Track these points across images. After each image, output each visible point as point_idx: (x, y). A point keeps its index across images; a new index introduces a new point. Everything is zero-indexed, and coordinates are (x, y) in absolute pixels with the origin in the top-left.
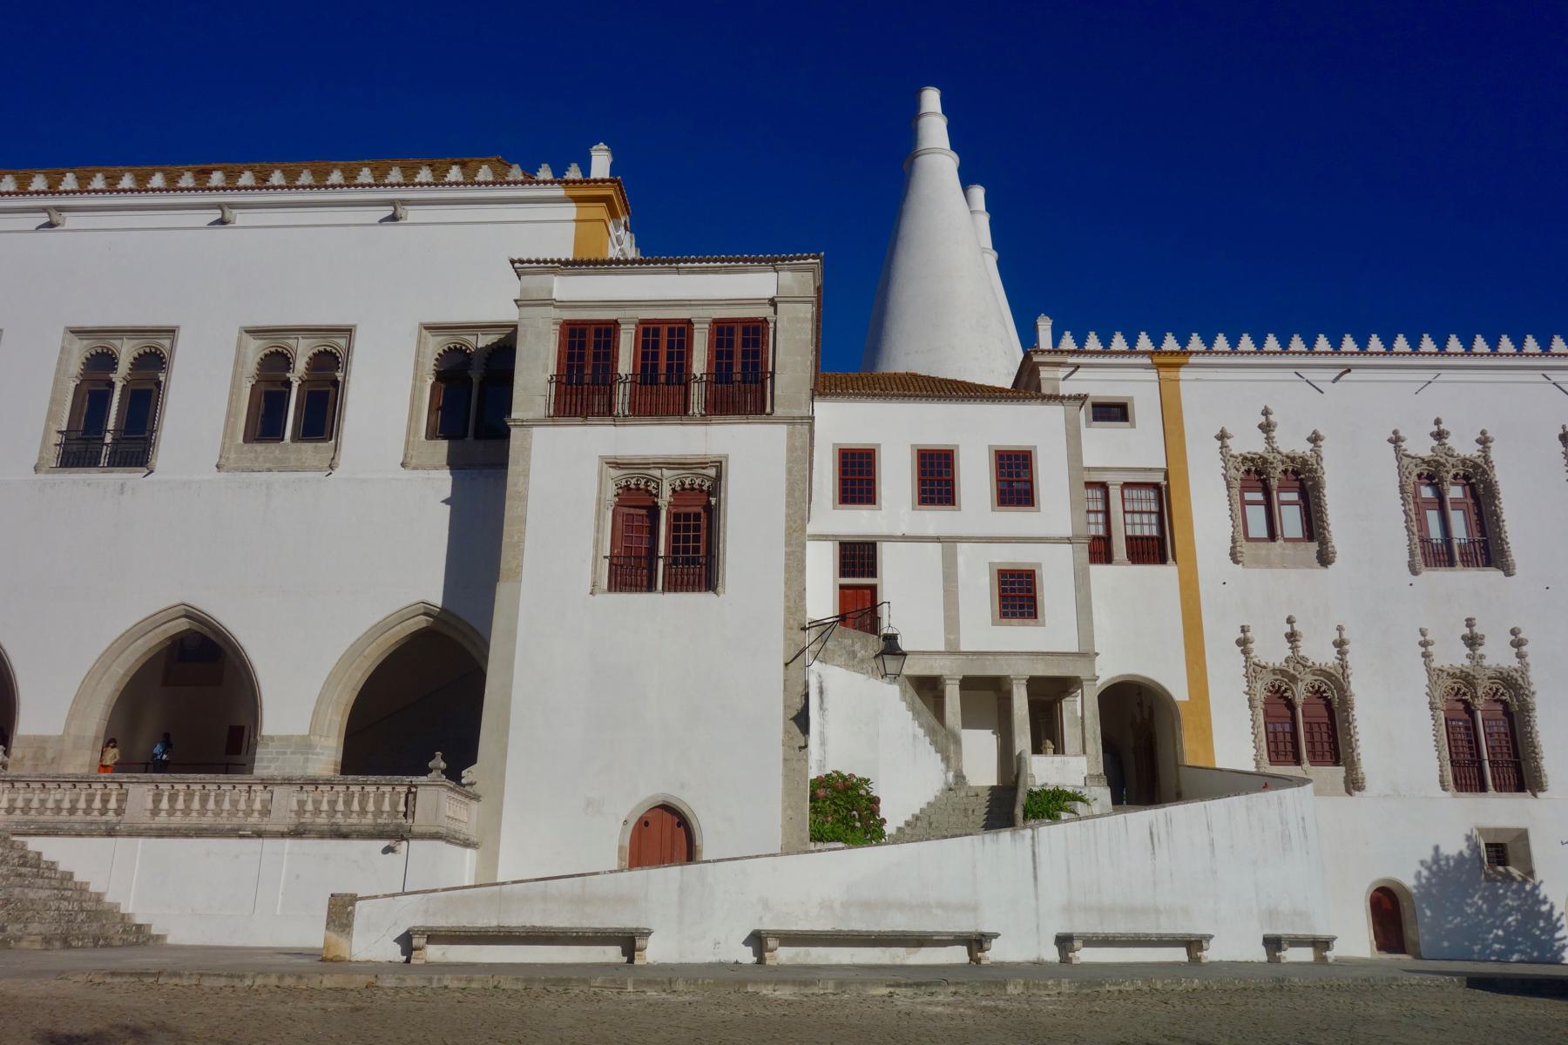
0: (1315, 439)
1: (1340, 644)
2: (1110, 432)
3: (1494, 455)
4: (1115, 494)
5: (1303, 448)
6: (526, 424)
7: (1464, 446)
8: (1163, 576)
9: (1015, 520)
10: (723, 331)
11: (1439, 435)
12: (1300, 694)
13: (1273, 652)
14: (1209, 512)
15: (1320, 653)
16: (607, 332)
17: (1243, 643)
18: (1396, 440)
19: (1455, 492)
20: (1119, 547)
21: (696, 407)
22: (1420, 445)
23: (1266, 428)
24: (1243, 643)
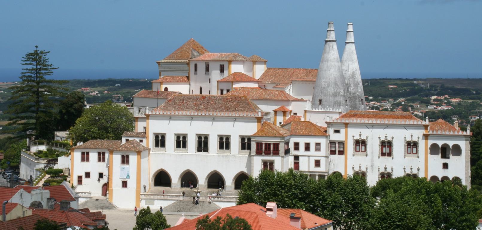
0: (367, 137)
1: (367, 169)
2: (337, 135)
3: (394, 140)
4: (337, 144)
5: (365, 138)
6: (253, 156)
7: (389, 139)
8: (342, 157)
9: (318, 154)
10: (274, 144)
14: (350, 147)
15: (363, 169)
16: (261, 144)
17: (353, 168)
18: (379, 138)
20: (337, 152)
21: (272, 154)
22: (383, 139)
23: (360, 135)
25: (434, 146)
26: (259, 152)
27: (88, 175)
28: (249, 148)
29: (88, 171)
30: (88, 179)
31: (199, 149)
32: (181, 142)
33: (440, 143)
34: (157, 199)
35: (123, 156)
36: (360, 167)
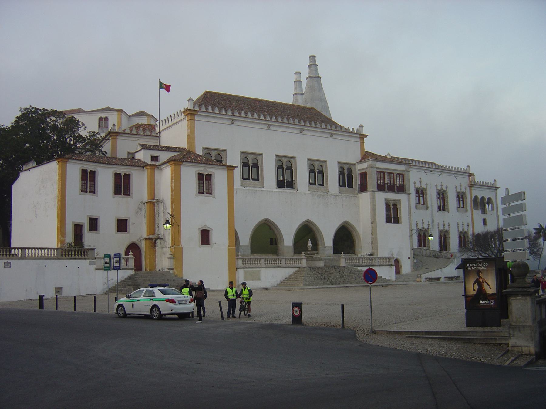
1: (429, 225)
11: (442, 185)
12: (422, 234)
13: (420, 227)
17: (417, 224)
19: (441, 196)
21: (396, 190)
22: (439, 188)
23: (420, 182)
24: (417, 224)
25: (476, 197)
26: (381, 188)
27: (94, 224)
28: (350, 185)
29: (94, 215)
30: (93, 234)
31: (280, 184)
32: (251, 167)
33: (479, 193)
34: (266, 268)
35: (200, 176)
36: (423, 223)
